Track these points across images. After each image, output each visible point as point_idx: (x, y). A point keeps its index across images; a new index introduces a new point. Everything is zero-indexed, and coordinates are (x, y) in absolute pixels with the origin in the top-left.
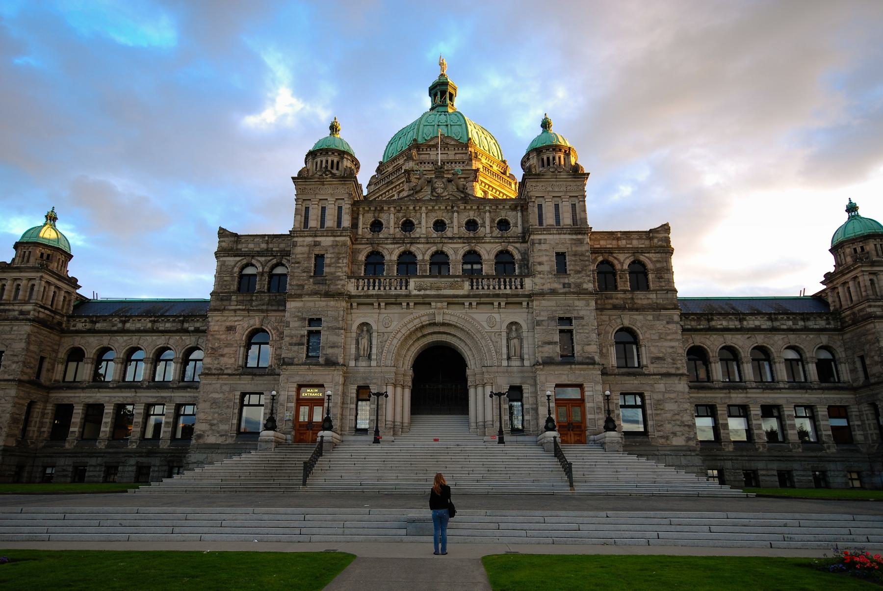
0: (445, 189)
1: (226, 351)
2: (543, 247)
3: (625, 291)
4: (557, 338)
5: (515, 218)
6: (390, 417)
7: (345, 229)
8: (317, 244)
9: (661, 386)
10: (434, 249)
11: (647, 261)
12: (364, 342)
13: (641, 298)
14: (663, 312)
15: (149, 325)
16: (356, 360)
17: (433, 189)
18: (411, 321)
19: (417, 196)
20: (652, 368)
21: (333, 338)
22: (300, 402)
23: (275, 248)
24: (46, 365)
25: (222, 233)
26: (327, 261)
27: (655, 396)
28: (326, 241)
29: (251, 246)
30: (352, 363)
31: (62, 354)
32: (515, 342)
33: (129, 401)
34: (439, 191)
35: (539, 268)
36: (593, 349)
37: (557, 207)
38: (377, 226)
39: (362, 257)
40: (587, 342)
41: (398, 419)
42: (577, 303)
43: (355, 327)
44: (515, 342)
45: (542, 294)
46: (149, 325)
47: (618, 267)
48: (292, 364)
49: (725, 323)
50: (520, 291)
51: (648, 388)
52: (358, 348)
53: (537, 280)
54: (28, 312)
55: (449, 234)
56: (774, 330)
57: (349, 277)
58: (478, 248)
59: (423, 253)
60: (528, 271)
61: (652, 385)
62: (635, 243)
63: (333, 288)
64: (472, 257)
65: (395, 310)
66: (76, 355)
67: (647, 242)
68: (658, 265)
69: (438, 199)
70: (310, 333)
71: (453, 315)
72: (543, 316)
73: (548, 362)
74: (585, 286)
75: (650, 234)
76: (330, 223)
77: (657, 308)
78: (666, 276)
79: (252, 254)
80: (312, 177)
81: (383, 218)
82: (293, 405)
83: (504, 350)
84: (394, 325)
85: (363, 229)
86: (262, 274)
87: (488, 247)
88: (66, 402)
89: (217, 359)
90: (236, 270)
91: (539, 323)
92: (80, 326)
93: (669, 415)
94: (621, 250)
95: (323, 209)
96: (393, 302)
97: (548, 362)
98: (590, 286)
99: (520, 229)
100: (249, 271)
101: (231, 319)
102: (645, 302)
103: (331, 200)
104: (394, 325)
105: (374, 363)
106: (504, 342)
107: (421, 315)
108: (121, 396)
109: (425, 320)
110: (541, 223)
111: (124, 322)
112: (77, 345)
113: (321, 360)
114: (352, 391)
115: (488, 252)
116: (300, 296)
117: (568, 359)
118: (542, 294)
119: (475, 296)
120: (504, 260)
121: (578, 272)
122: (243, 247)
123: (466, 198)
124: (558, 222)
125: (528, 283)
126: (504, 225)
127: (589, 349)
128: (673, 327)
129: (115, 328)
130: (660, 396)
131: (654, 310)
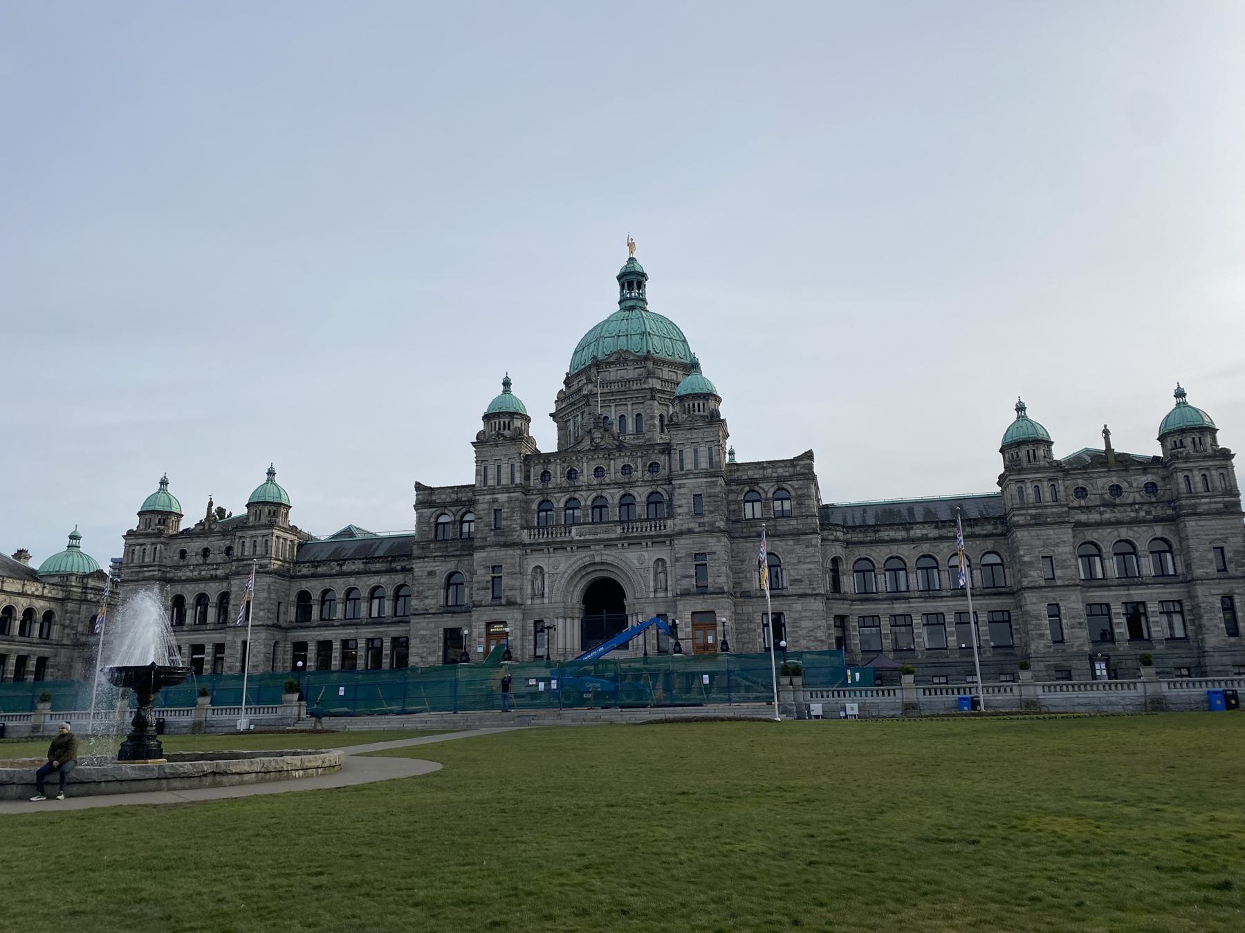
0: (602, 438)
1: (430, 593)
2: (683, 491)
3: (768, 519)
4: (693, 572)
5: (662, 460)
6: (561, 646)
7: (517, 486)
8: (495, 501)
9: (798, 606)
10: (594, 495)
11: (789, 488)
12: (538, 583)
13: (783, 526)
14: (802, 537)
15: (362, 567)
16: (532, 598)
17: (592, 440)
18: (575, 562)
19: (579, 447)
20: (791, 590)
21: (511, 582)
22: (489, 636)
23: (461, 499)
24: (282, 609)
25: (419, 487)
26: (504, 515)
27: (793, 615)
28: (503, 497)
29: (443, 497)
30: (529, 602)
32: (662, 576)
33: (352, 637)
34: (598, 441)
35: (679, 510)
36: (723, 579)
37: (696, 450)
38: (545, 476)
39: (535, 506)
40: (719, 575)
41: (569, 646)
42: (710, 540)
43: (530, 570)
44: (662, 576)
45: (681, 533)
46: (362, 567)
47: (763, 496)
48: (480, 606)
49: (892, 533)
50: (663, 532)
51: (786, 608)
52: (533, 588)
53: (678, 521)
54: (266, 566)
55: (607, 480)
56: (941, 538)
57: (523, 528)
58: (631, 492)
60: (671, 516)
61: (790, 605)
63: (510, 539)
64: (627, 502)
65: (562, 553)
67: (791, 470)
68: (800, 492)
69: (597, 448)
70: (493, 578)
71: (609, 555)
72: (682, 553)
73: (685, 594)
74: (717, 524)
75: (793, 462)
77: (796, 534)
78: (807, 502)
79: (444, 505)
80: (488, 441)
81: (551, 468)
82: (483, 640)
83: (652, 584)
84: (562, 567)
85: (535, 481)
86: (454, 523)
87: (640, 490)
88: (301, 640)
89: (422, 600)
90: (432, 520)
91: (677, 560)
92: (305, 571)
93: (804, 632)
94: (766, 479)
95: (499, 467)
96: (559, 547)
97: (685, 594)
98: (721, 524)
99: (667, 472)
100: (442, 519)
101: (431, 565)
102: (786, 528)
103: (505, 460)
104: (562, 567)
105: (546, 601)
106: (652, 577)
107: (582, 557)
108: (348, 633)
109: (587, 561)
110: (682, 469)
111: (341, 565)
112: (304, 588)
113: (503, 601)
114: (530, 626)
115: (641, 494)
116: (482, 548)
117: (702, 590)
118: (681, 533)
119: (625, 538)
120: (654, 500)
121: (711, 512)
122: (437, 499)
123: (620, 447)
124: (696, 466)
125: (670, 522)
126: (654, 467)
127: (719, 580)
128: (811, 550)
129: (334, 572)
130: (797, 615)
131: (793, 534)
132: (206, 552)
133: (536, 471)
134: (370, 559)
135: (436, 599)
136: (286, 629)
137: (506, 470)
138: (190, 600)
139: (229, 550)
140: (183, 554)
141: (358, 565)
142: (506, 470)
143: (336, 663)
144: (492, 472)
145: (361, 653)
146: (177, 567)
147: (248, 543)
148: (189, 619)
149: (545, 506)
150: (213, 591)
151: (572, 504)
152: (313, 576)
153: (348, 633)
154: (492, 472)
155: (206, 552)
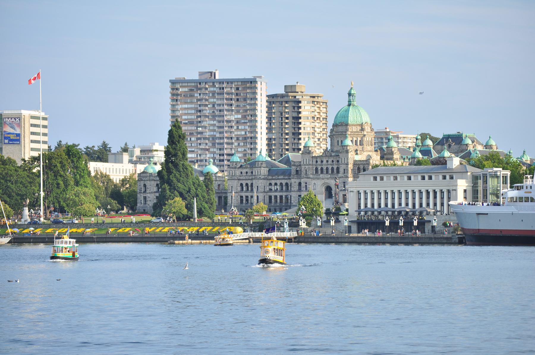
28: (307, 167)
31: (268, 184)
38: (317, 162)
39: (314, 169)
59: (325, 168)
62: (365, 163)
66: (270, 184)
76: (308, 163)
79: (297, 166)
85: (314, 163)
96: (318, 179)
107: (323, 181)
108: (281, 194)
115: (335, 167)
122: (296, 164)
126: (338, 161)
132: (247, 173)
133: (315, 160)
134: (285, 175)
135: (296, 188)
136: (267, 192)
137: (308, 160)
138: (244, 185)
139: (252, 172)
140: (241, 173)
141: (282, 177)
142: (308, 160)
143: (278, 201)
144: (305, 161)
145: (284, 199)
146: (240, 176)
147: (256, 172)
148: (244, 189)
149: (317, 169)
150: (249, 182)
151: (322, 169)
152: (272, 179)
153: (281, 194)
154: (305, 161)
155: (247, 173)
